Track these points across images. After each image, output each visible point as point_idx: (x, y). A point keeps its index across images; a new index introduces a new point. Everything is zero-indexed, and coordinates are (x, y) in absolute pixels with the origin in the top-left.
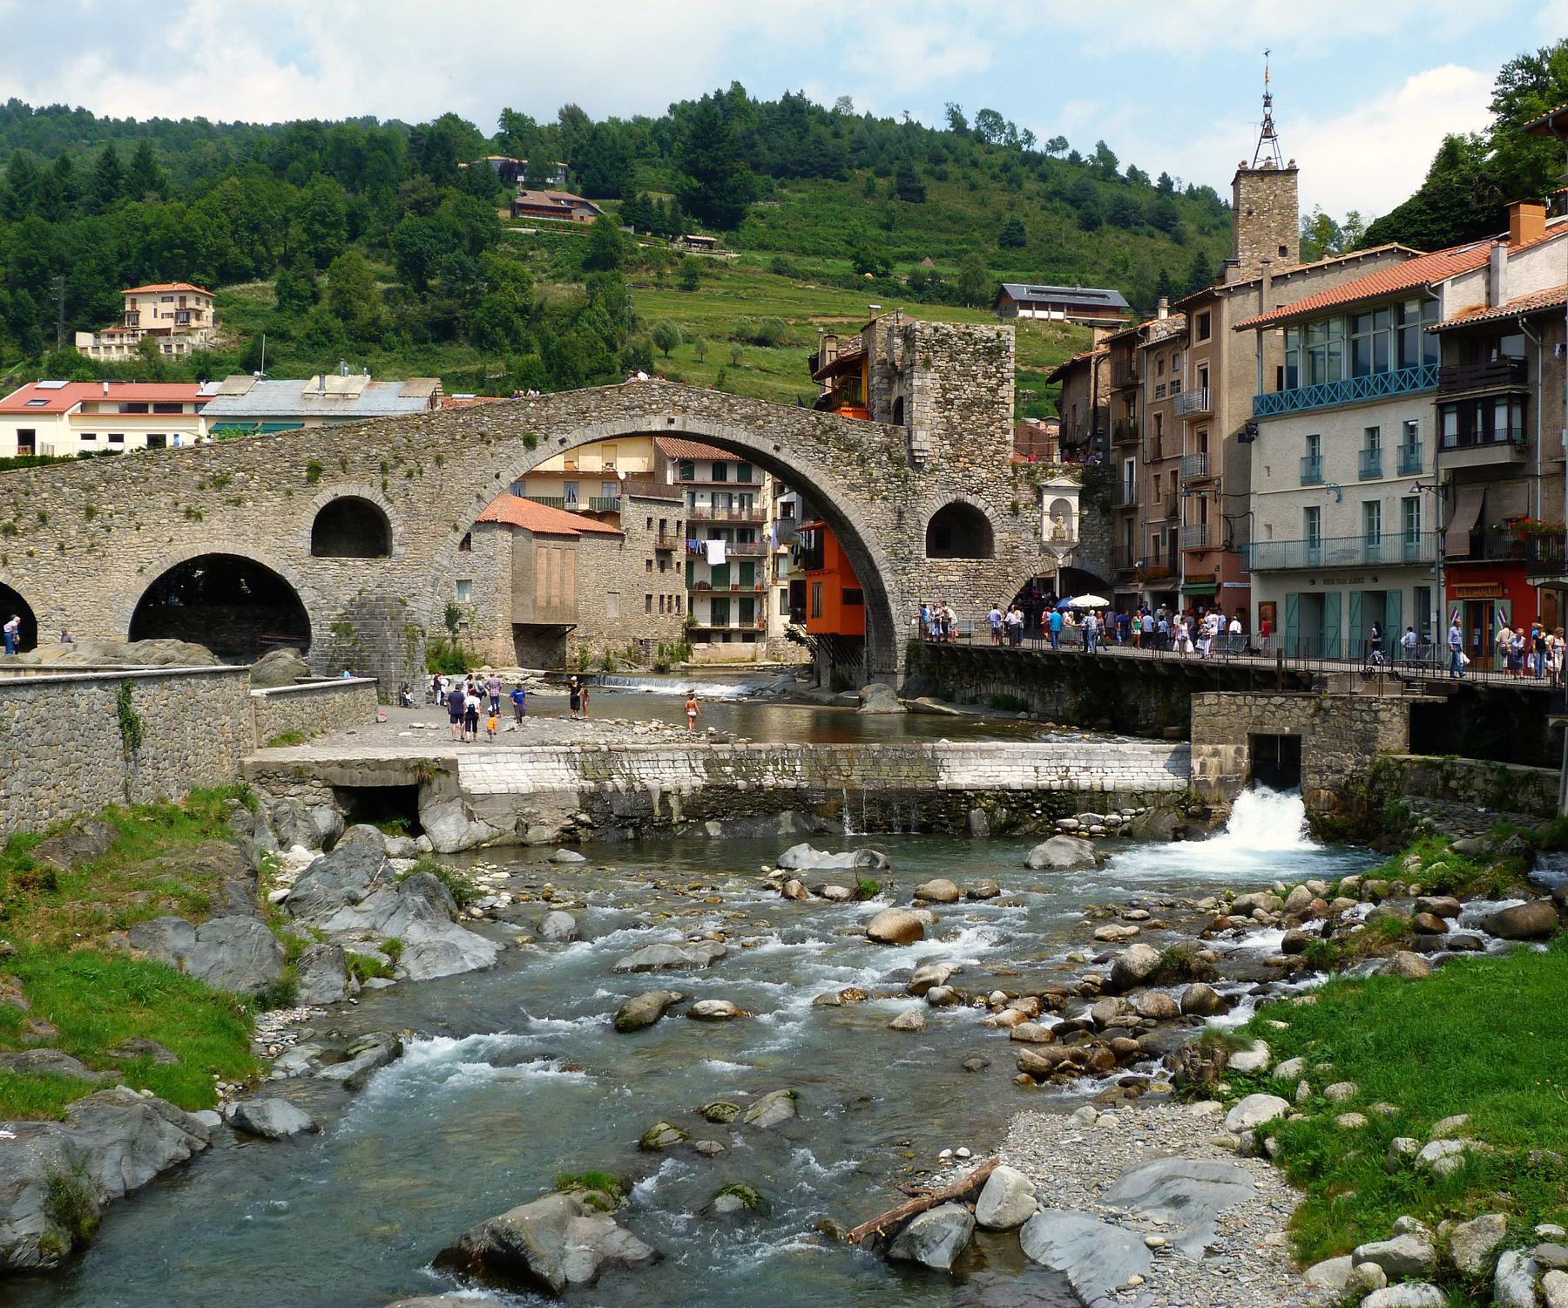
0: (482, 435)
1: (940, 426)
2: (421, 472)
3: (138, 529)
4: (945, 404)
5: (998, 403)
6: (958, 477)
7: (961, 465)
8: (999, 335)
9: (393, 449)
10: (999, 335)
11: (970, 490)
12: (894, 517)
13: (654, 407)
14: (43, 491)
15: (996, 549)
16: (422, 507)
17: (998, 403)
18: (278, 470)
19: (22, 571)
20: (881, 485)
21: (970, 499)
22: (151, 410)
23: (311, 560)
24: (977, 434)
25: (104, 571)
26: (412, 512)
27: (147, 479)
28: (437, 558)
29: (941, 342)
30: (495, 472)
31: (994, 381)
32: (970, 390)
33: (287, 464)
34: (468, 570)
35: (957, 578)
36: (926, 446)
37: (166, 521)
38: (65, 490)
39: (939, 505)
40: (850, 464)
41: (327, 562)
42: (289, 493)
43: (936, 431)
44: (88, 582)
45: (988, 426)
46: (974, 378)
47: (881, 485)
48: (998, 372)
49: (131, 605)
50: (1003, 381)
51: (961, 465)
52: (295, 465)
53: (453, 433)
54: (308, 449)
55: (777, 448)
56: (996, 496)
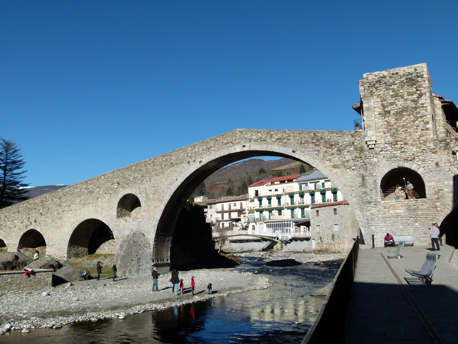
0: (171, 163)
1: (383, 127)
2: (150, 181)
3: (71, 211)
4: (385, 113)
5: (419, 107)
6: (398, 153)
7: (398, 146)
8: (416, 70)
9: (142, 173)
10: (416, 70)
11: (406, 160)
12: (360, 180)
13: (237, 141)
14: (49, 200)
15: (427, 192)
16: (151, 196)
17: (419, 107)
18: (108, 186)
19: (43, 228)
20: (351, 163)
21: (407, 165)
22: (286, 181)
23: (117, 219)
24: (406, 127)
25: (62, 227)
26: (148, 198)
27: (74, 193)
28: (156, 216)
29: (379, 82)
30: (176, 179)
31: (415, 96)
32: (400, 103)
33: (110, 184)
34: (336, 221)
35: (402, 211)
36: (374, 138)
37: (78, 208)
38: (54, 200)
39: (386, 170)
40: (333, 154)
41: (122, 220)
42: (111, 194)
43: (381, 130)
44: (58, 231)
45: (414, 121)
46: (402, 97)
47: (351, 163)
48: (417, 90)
49: (68, 238)
50: (420, 96)
51: (398, 146)
52: (113, 184)
53: (162, 165)
54: (117, 178)
55: (294, 152)
56: (424, 161)
